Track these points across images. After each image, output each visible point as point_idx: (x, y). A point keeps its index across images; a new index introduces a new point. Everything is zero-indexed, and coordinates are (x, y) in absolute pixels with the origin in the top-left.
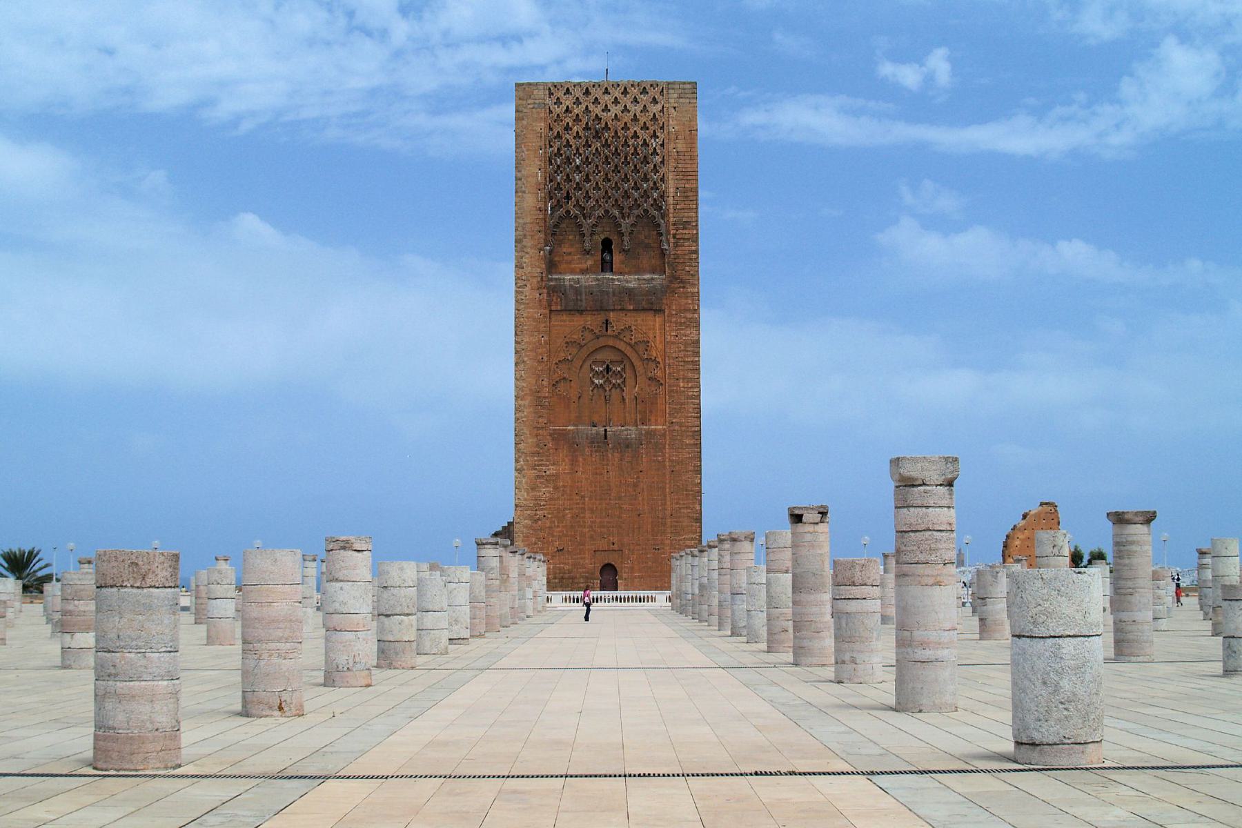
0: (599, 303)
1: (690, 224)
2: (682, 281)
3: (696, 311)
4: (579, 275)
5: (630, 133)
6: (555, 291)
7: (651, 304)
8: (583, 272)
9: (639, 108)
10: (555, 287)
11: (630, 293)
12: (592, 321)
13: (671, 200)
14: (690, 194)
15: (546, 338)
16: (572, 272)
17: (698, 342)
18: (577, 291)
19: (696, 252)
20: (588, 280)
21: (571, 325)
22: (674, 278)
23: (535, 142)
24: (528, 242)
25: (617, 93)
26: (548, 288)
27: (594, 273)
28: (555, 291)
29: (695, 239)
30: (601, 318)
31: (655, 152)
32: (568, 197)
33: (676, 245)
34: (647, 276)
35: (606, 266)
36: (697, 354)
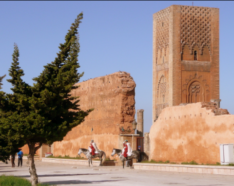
0: (194, 69)
1: (217, 48)
2: (215, 64)
3: (218, 72)
4: (189, 62)
5: (202, 21)
6: (183, 65)
7: (207, 70)
8: (190, 60)
9: (204, 14)
10: (183, 64)
11: (201, 66)
12: (192, 74)
13: (212, 41)
14: (217, 40)
15: (180, 78)
16: (187, 60)
17: (218, 81)
18: (189, 65)
19: (219, 56)
20: (192, 62)
21: (186, 75)
22: (213, 63)
23: (178, 22)
24: (176, 51)
25: (199, 10)
26: (181, 64)
27: (192, 60)
28: (183, 65)
29: (218, 52)
30: (194, 74)
31: (208, 28)
32: (186, 39)
33: (214, 53)
34: (206, 62)
35: (195, 59)
36: (219, 84)
